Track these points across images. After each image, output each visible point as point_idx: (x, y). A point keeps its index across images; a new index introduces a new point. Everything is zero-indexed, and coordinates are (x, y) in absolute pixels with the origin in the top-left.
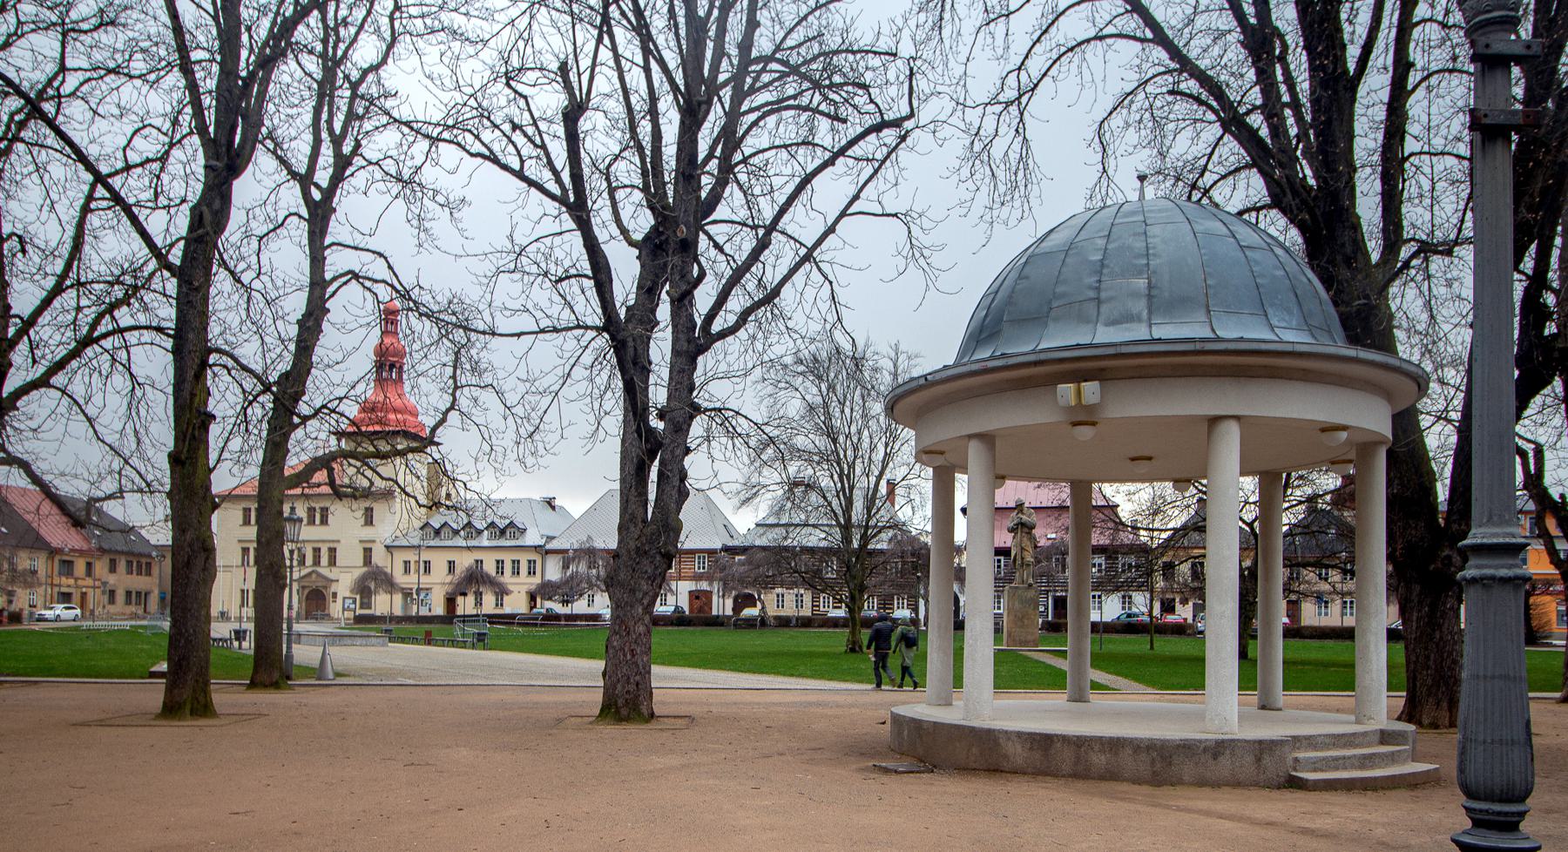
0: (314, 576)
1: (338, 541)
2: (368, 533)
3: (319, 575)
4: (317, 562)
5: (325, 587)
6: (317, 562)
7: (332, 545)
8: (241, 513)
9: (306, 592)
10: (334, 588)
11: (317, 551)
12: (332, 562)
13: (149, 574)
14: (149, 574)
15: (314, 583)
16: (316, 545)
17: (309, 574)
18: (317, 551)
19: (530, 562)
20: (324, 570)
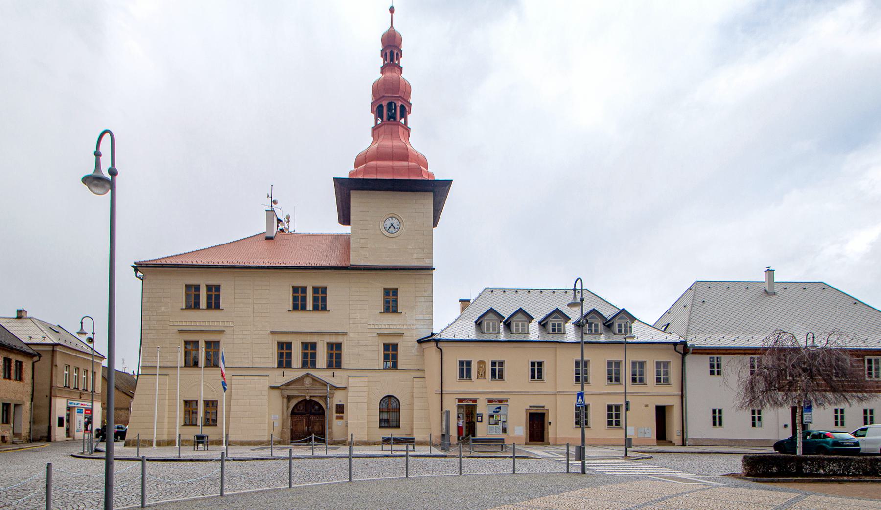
0: (308, 381)
1: (345, 334)
2: (390, 323)
3: (315, 380)
4: (309, 360)
5: (325, 398)
6: (309, 360)
7: (334, 339)
8: (184, 290)
9: (294, 403)
10: (338, 398)
11: (310, 349)
12: (335, 362)
13: (20, 379)
14: (20, 379)
15: (309, 392)
16: (309, 339)
17: (300, 380)
18: (310, 349)
19: (658, 364)
20: (322, 373)
